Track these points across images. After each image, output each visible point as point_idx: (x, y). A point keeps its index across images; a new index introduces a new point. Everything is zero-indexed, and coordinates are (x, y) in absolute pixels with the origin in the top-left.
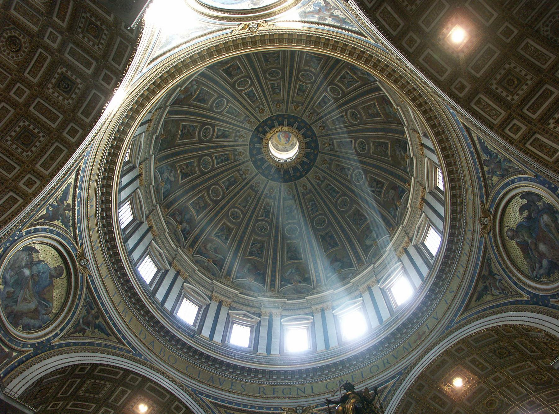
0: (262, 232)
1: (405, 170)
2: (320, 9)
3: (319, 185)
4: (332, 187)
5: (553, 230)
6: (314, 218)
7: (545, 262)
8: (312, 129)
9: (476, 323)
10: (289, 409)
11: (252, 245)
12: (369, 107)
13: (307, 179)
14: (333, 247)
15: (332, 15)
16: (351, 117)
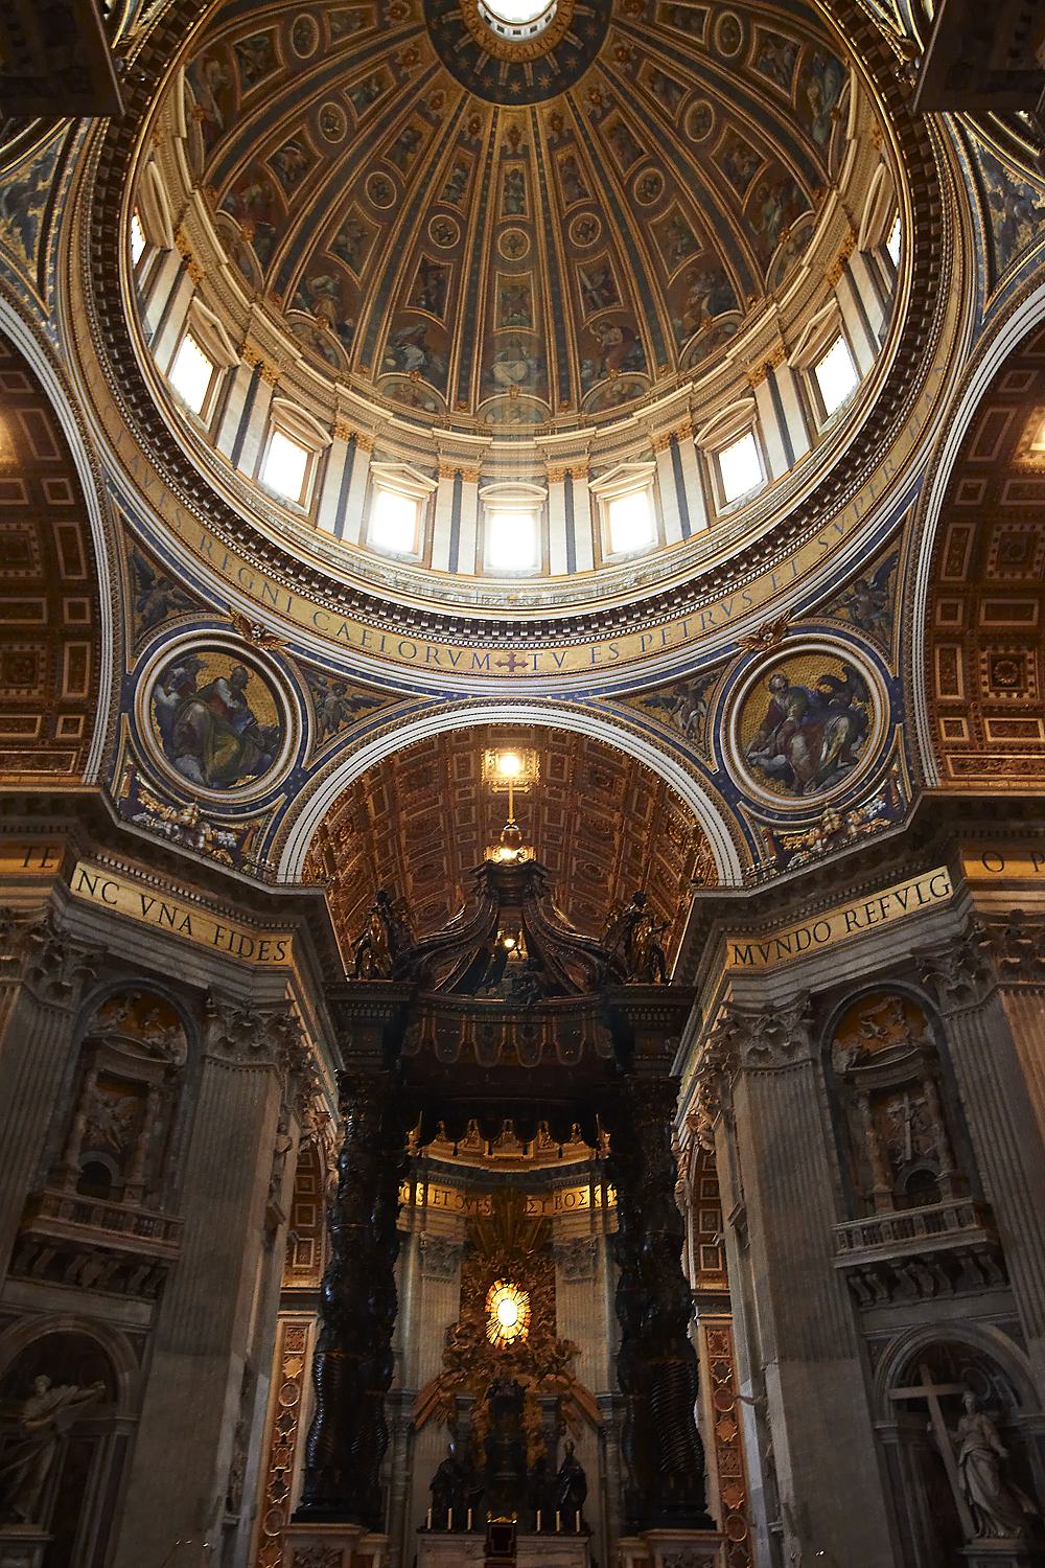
0: (325, 132)
1: (682, 333)
2: (1021, 198)
3: (503, 149)
4: (523, 187)
5: (834, 745)
6: (440, 209)
7: (781, 759)
8: (606, 32)
9: (616, 729)
10: (241, 618)
11: (287, 144)
12: (743, 146)
13: (496, 115)
14: (429, 307)
15: (1012, 224)
16: (695, 116)
